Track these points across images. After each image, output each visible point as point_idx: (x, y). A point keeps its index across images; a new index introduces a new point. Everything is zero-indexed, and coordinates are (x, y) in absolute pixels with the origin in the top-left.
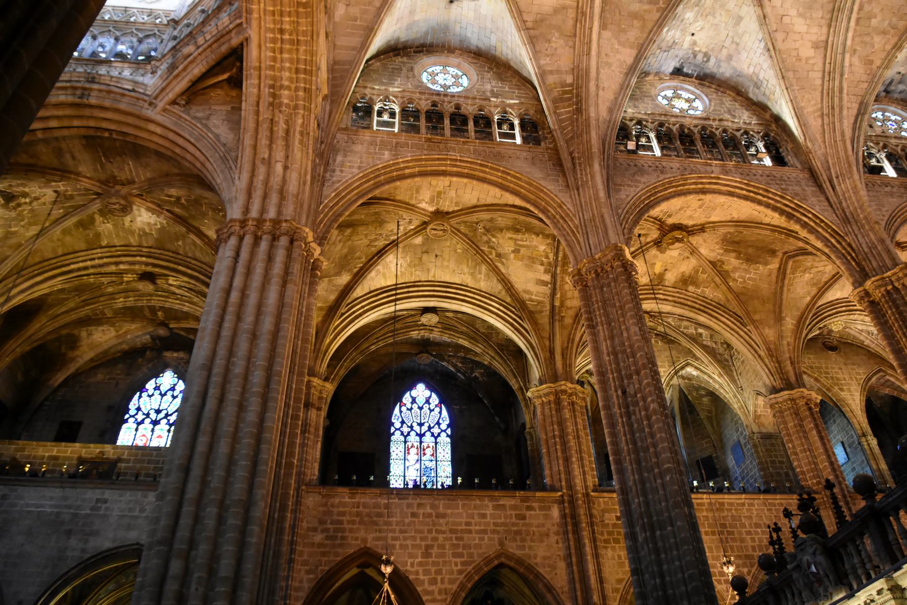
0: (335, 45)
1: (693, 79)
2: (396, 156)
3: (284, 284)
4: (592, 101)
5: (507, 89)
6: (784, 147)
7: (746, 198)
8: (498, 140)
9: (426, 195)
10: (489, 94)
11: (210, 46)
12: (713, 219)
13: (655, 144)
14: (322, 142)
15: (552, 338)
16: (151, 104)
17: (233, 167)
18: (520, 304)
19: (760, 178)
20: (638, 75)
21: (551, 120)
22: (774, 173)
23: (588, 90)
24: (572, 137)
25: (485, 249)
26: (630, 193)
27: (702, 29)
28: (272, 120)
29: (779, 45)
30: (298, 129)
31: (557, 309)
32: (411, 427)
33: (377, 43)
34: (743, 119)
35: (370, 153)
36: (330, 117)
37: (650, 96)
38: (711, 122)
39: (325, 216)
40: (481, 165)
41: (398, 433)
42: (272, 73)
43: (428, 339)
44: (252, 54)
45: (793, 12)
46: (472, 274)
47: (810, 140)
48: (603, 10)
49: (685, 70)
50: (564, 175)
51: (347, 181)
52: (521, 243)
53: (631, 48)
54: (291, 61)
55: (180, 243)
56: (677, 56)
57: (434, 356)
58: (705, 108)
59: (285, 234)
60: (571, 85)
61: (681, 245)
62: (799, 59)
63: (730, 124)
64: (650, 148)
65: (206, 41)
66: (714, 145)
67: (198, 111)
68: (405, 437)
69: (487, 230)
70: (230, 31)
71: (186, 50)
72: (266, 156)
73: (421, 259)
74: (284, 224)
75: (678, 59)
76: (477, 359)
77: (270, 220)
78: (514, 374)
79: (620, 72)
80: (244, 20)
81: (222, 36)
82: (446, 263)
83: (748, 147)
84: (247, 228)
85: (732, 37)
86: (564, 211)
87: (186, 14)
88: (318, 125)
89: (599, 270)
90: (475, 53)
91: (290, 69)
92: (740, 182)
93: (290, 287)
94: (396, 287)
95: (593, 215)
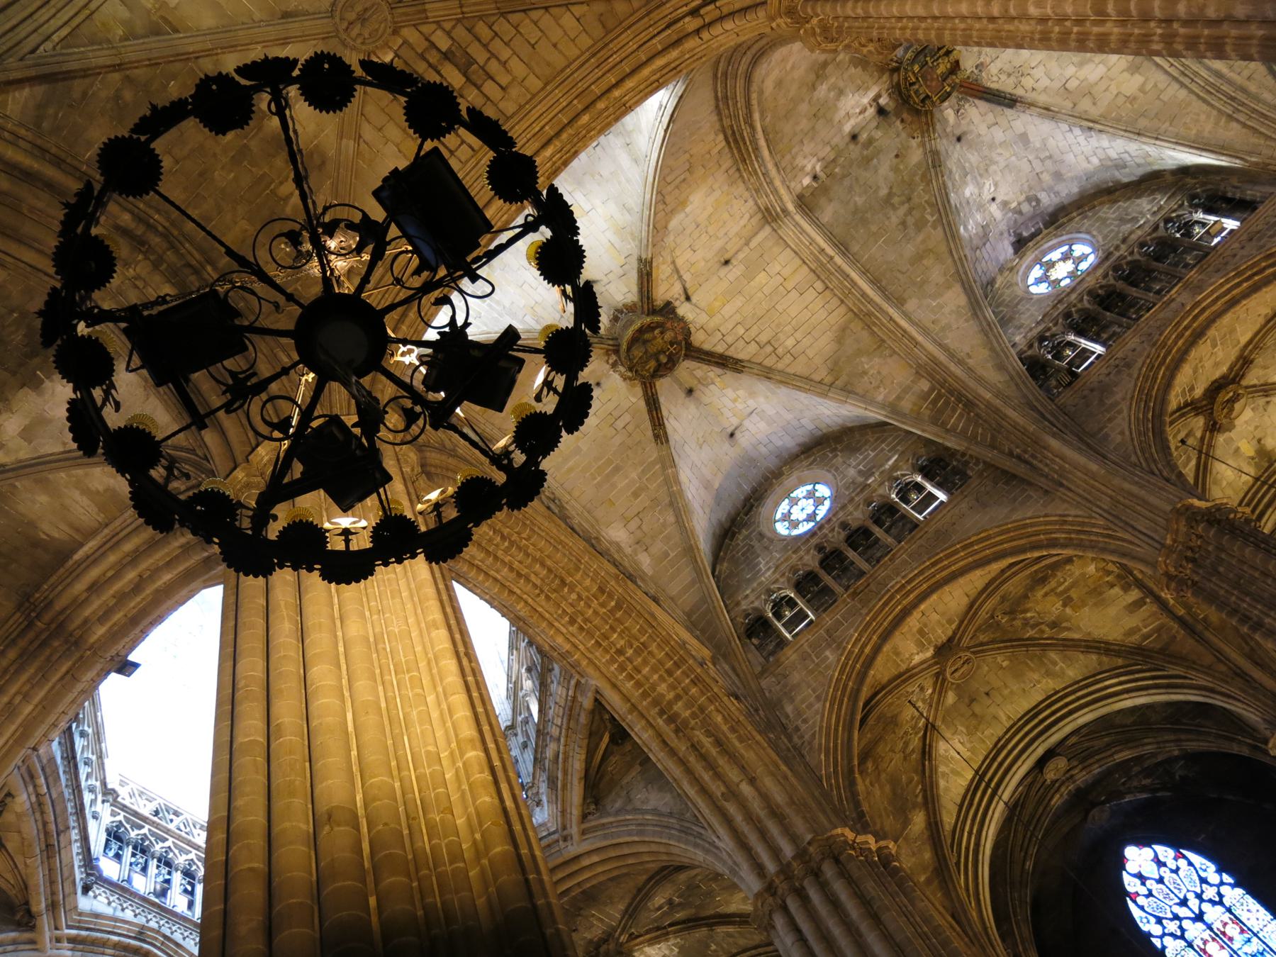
0: (672, 599)
1: (1045, 232)
2: (840, 647)
3: (875, 919)
4: (972, 384)
5: (872, 454)
6: (1229, 189)
7: (1256, 288)
8: (920, 517)
9: (910, 649)
10: (861, 479)
11: (568, 728)
12: (1244, 340)
13: (1085, 343)
14: (757, 710)
15: (1220, 656)
16: (565, 839)
17: (702, 831)
18: (1138, 654)
19: (1244, 252)
20: (987, 298)
21: (951, 443)
22: (1254, 229)
23: (956, 378)
24: (993, 437)
25: (1031, 633)
26: (1121, 425)
27: (996, 185)
28: (693, 745)
29: (1094, 112)
30: (725, 728)
31: (1188, 618)
32: (1176, 917)
33: (704, 544)
34: (1147, 210)
35: (812, 672)
36: (738, 675)
37: (1022, 299)
38: (1117, 254)
39: (838, 788)
40: (933, 565)
41: (1168, 941)
42: (649, 699)
43: (1078, 790)
44: (614, 700)
45: (1071, 70)
46: (1048, 674)
47: (1250, 153)
48: (882, 290)
49: (1025, 234)
50: (1030, 484)
51: (821, 728)
52: (1061, 589)
53: (949, 288)
54: (654, 670)
55: (713, 947)
56: (1002, 234)
57: (1107, 801)
58: (1091, 244)
59: (823, 859)
60: (932, 389)
61: (1242, 401)
62: (1132, 99)
63: (1139, 233)
64: (1085, 354)
65: (561, 727)
66: (1149, 271)
67: (614, 801)
68: (1182, 937)
69: (1012, 613)
70: (574, 698)
71: (549, 753)
72: (723, 789)
73: (974, 715)
74: (811, 849)
75: (1006, 235)
76: (1160, 759)
77: (794, 858)
78: (1226, 738)
79: (967, 321)
80: (577, 677)
81: (571, 709)
82: (1006, 692)
83: (1188, 234)
84: (780, 892)
85: (1037, 158)
86: (1072, 524)
87: (514, 710)
88: (737, 698)
89: (1189, 554)
90: (803, 453)
91: (662, 679)
92: (1227, 281)
93: (885, 917)
94: (980, 775)
95: (1111, 497)
